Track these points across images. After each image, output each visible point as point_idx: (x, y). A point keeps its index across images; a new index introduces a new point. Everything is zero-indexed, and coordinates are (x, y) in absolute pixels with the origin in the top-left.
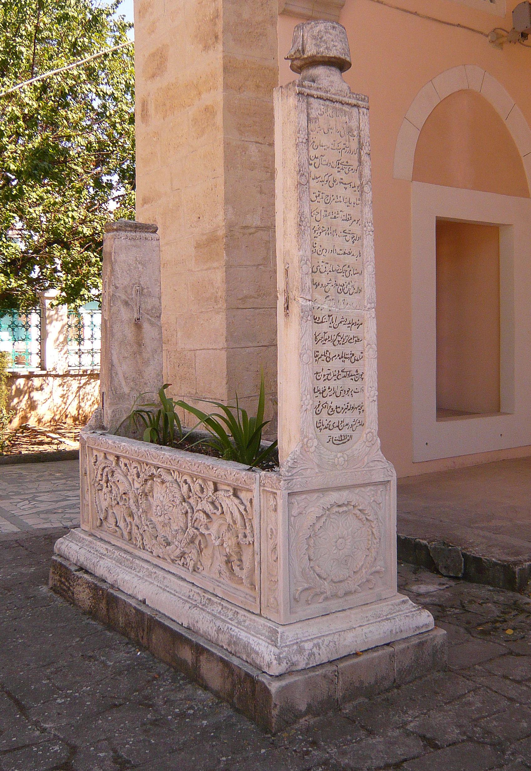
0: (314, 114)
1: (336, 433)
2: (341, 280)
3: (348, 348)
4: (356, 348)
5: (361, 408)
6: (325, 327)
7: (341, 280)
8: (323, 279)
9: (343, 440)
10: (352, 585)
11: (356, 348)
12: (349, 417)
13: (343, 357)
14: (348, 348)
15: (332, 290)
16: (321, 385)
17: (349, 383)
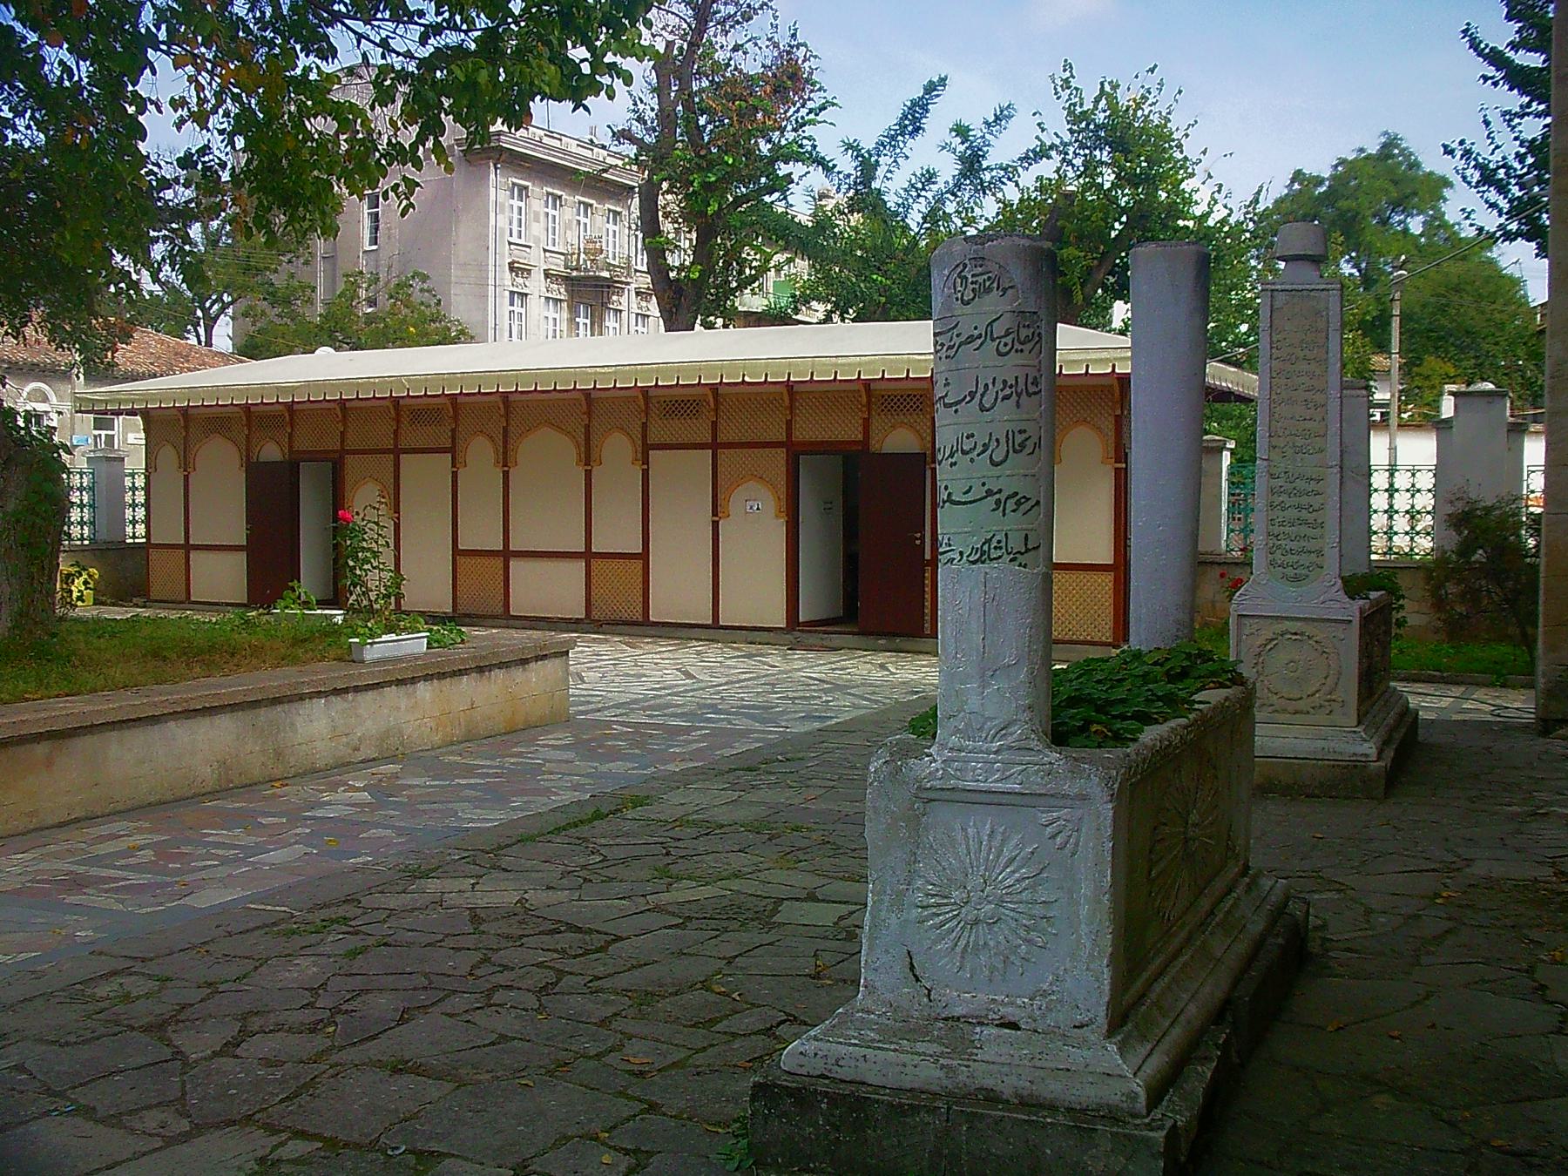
0: (1277, 304)
1: (1290, 572)
2: (1299, 442)
3: (1304, 500)
4: (1316, 501)
5: (1320, 553)
6: (1280, 482)
7: (1299, 442)
8: (1281, 442)
9: (1297, 579)
10: (1301, 705)
11: (1316, 501)
12: (1305, 559)
13: (1299, 507)
14: (1304, 500)
15: (1290, 452)
16: (1276, 530)
17: (1304, 530)
